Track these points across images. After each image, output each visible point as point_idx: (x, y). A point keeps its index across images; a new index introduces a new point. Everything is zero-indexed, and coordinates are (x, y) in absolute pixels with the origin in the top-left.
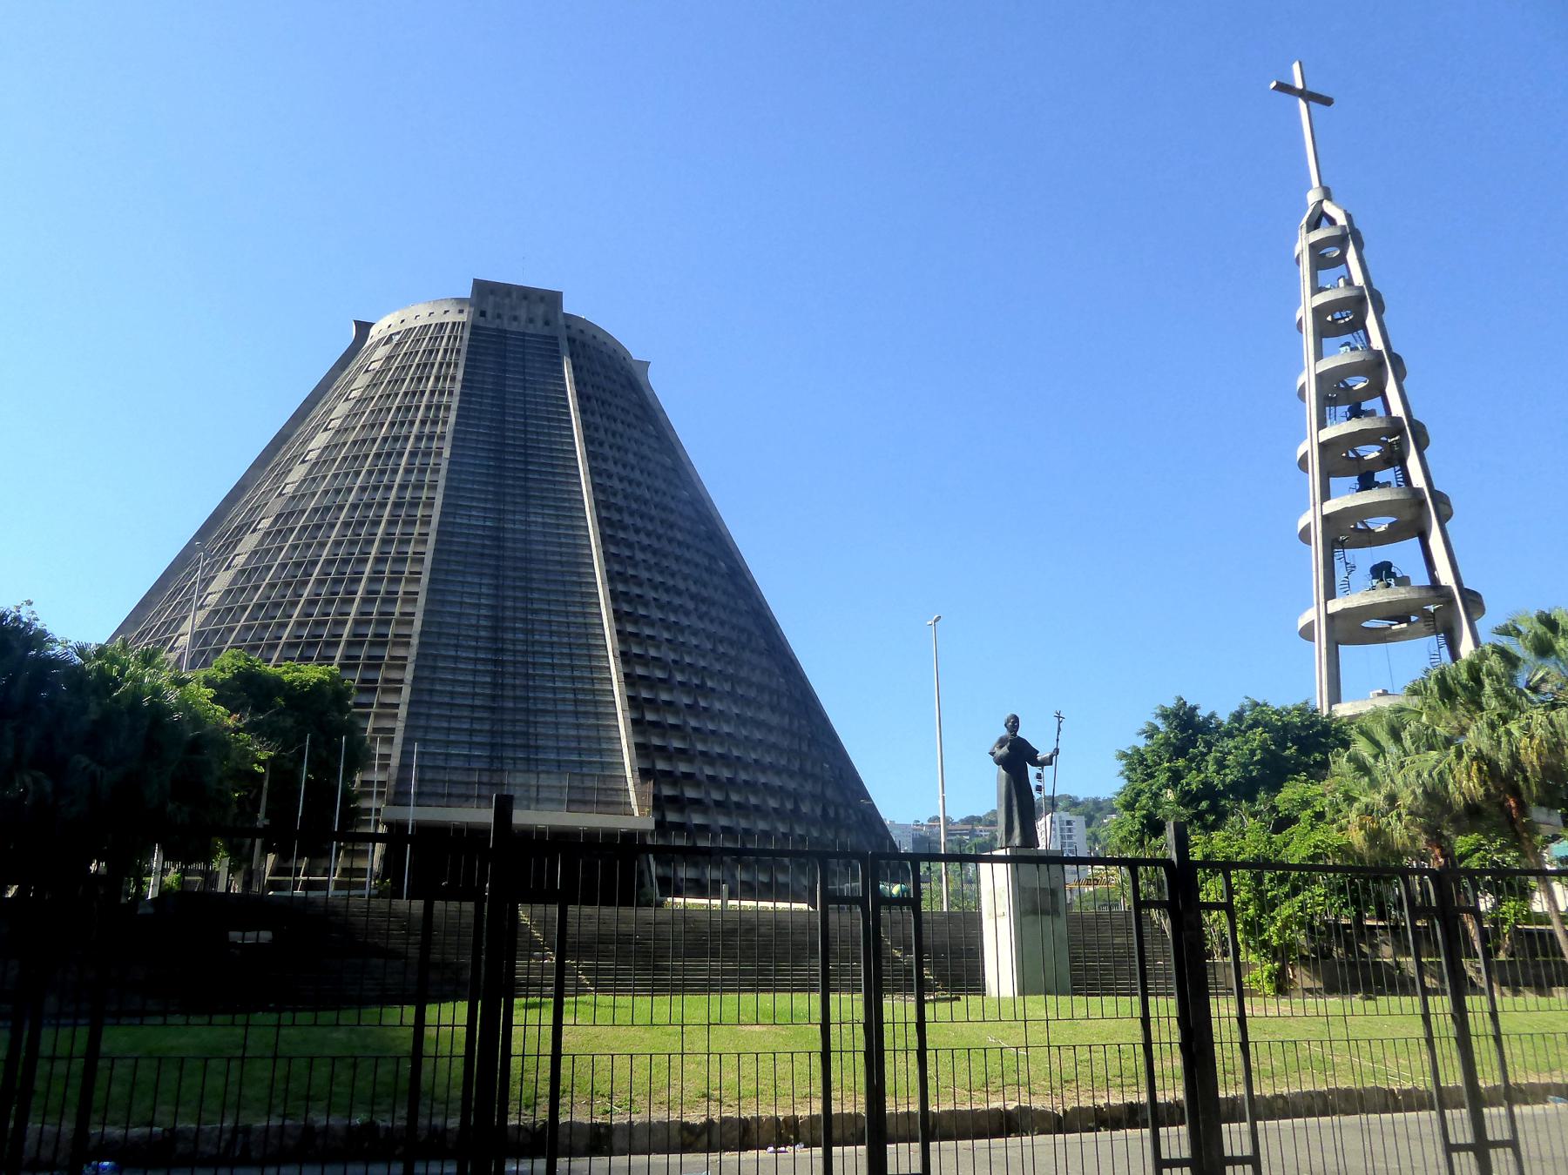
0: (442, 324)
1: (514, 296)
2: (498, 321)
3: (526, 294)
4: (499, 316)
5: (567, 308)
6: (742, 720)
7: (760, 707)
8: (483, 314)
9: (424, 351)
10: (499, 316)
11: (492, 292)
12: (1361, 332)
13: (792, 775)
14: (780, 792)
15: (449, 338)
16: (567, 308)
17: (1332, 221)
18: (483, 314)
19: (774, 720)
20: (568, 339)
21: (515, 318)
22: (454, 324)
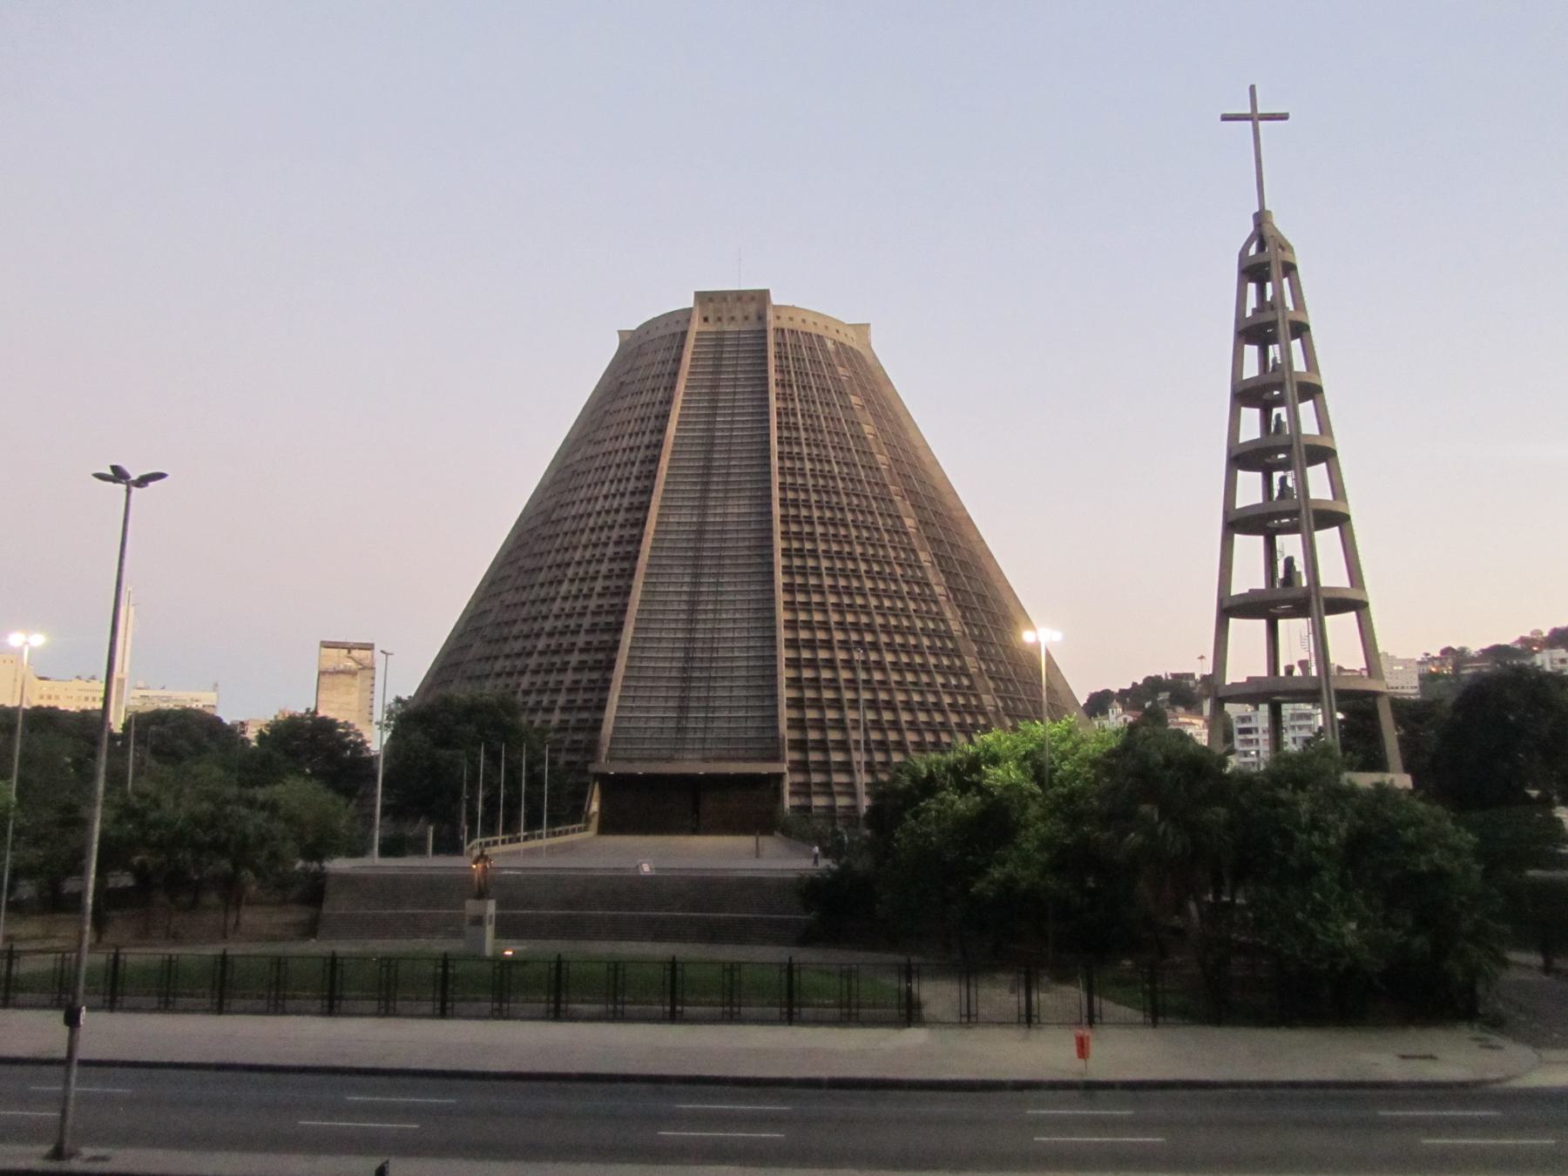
0: (674, 334)
1: (729, 299)
2: (719, 324)
3: (740, 296)
4: (720, 319)
5: (776, 300)
8: (706, 320)
10: (720, 319)
11: (711, 300)
21: (733, 318)
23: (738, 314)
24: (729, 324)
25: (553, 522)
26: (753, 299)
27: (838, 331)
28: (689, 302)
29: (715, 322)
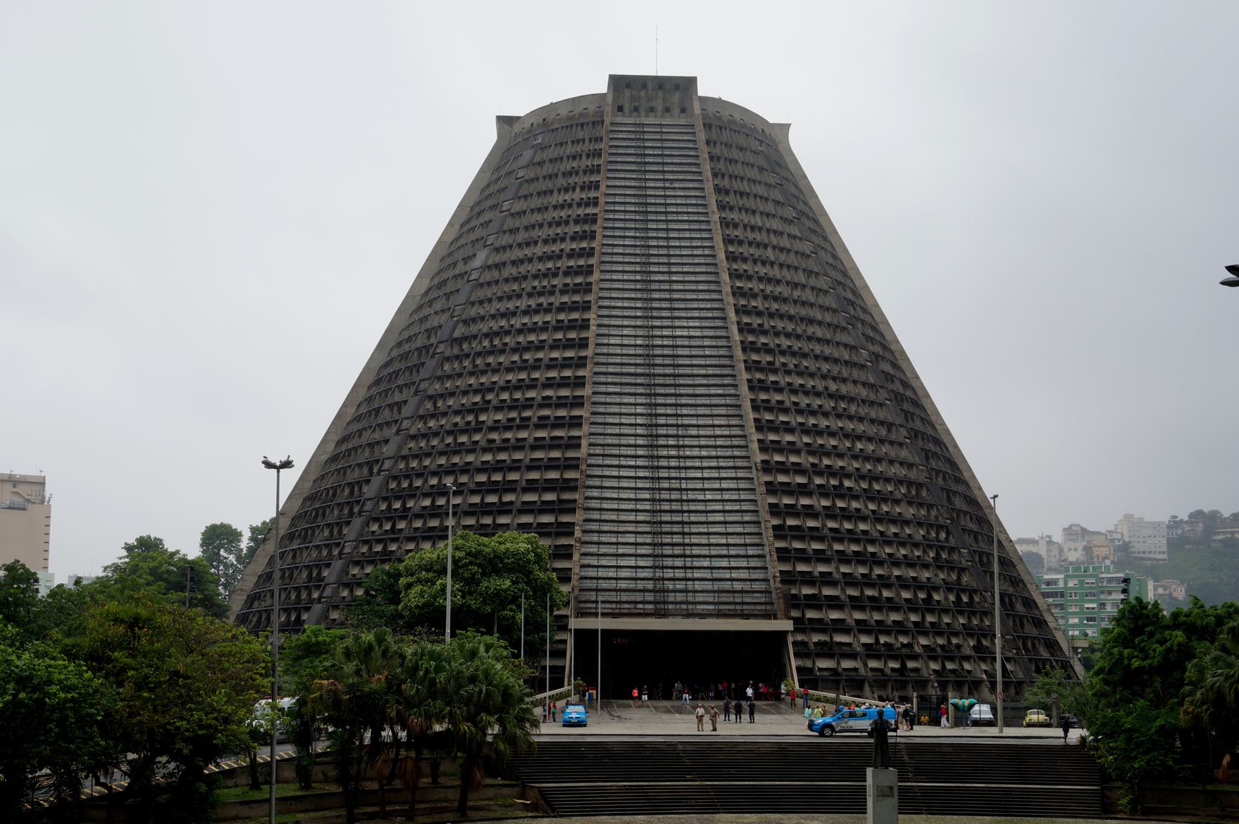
1: (650, 86)
3: (661, 83)
4: (636, 109)
5: (703, 90)
6: (878, 518)
7: (897, 502)
8: (620, 109)
10: (636, 109)
11: (628, 86)
13: (926, 566)
14: (915, 584)
16: (703, 90)
19: (909, 512)
20: (704, 125)
21: (652, 109)
23: (659, 104)
24: (647, 116)
25: (456, 340)
26: (677, 87)
27: (763, 130)
28: (602, 87)
29: (631, 112)
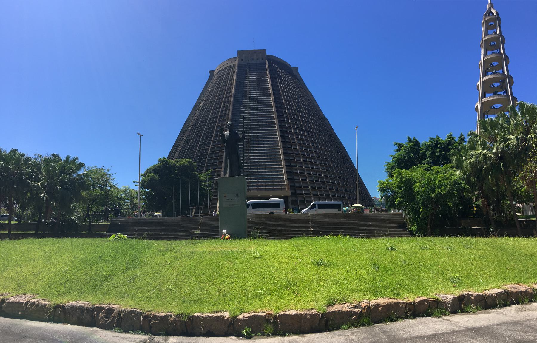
8: (242, 60)
9: (226, 74)
12: (498, 50)
15: (233, 68)
17: (493, 14)
18: (242, 60)
22: (234, 64)
